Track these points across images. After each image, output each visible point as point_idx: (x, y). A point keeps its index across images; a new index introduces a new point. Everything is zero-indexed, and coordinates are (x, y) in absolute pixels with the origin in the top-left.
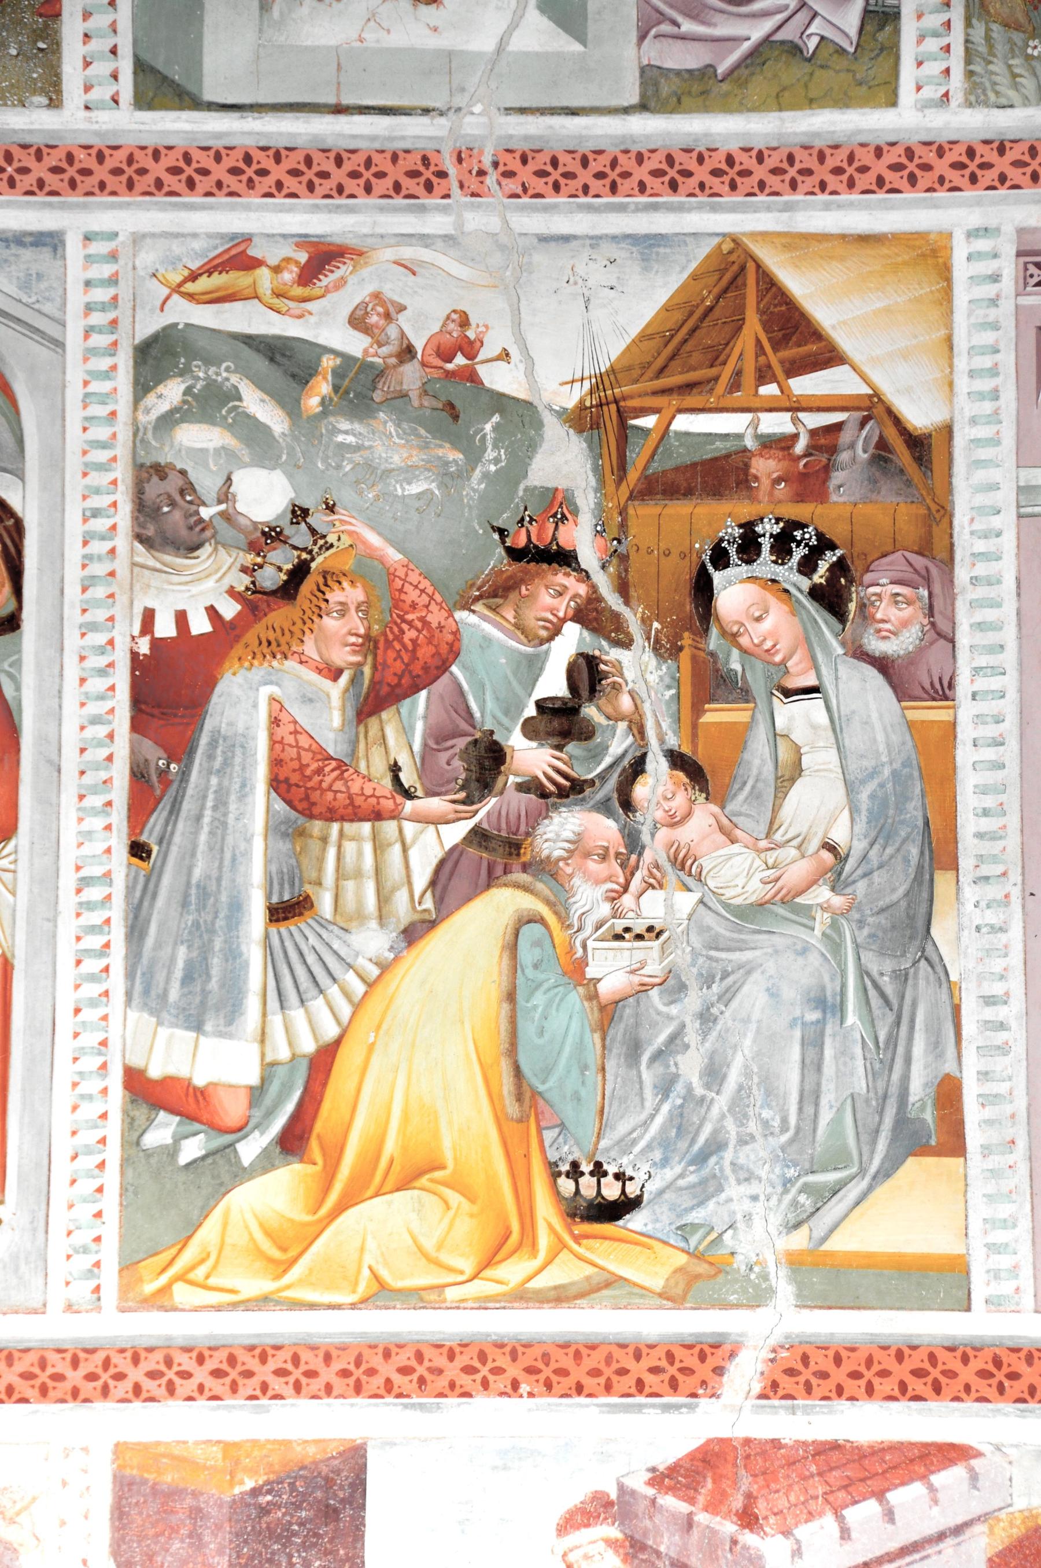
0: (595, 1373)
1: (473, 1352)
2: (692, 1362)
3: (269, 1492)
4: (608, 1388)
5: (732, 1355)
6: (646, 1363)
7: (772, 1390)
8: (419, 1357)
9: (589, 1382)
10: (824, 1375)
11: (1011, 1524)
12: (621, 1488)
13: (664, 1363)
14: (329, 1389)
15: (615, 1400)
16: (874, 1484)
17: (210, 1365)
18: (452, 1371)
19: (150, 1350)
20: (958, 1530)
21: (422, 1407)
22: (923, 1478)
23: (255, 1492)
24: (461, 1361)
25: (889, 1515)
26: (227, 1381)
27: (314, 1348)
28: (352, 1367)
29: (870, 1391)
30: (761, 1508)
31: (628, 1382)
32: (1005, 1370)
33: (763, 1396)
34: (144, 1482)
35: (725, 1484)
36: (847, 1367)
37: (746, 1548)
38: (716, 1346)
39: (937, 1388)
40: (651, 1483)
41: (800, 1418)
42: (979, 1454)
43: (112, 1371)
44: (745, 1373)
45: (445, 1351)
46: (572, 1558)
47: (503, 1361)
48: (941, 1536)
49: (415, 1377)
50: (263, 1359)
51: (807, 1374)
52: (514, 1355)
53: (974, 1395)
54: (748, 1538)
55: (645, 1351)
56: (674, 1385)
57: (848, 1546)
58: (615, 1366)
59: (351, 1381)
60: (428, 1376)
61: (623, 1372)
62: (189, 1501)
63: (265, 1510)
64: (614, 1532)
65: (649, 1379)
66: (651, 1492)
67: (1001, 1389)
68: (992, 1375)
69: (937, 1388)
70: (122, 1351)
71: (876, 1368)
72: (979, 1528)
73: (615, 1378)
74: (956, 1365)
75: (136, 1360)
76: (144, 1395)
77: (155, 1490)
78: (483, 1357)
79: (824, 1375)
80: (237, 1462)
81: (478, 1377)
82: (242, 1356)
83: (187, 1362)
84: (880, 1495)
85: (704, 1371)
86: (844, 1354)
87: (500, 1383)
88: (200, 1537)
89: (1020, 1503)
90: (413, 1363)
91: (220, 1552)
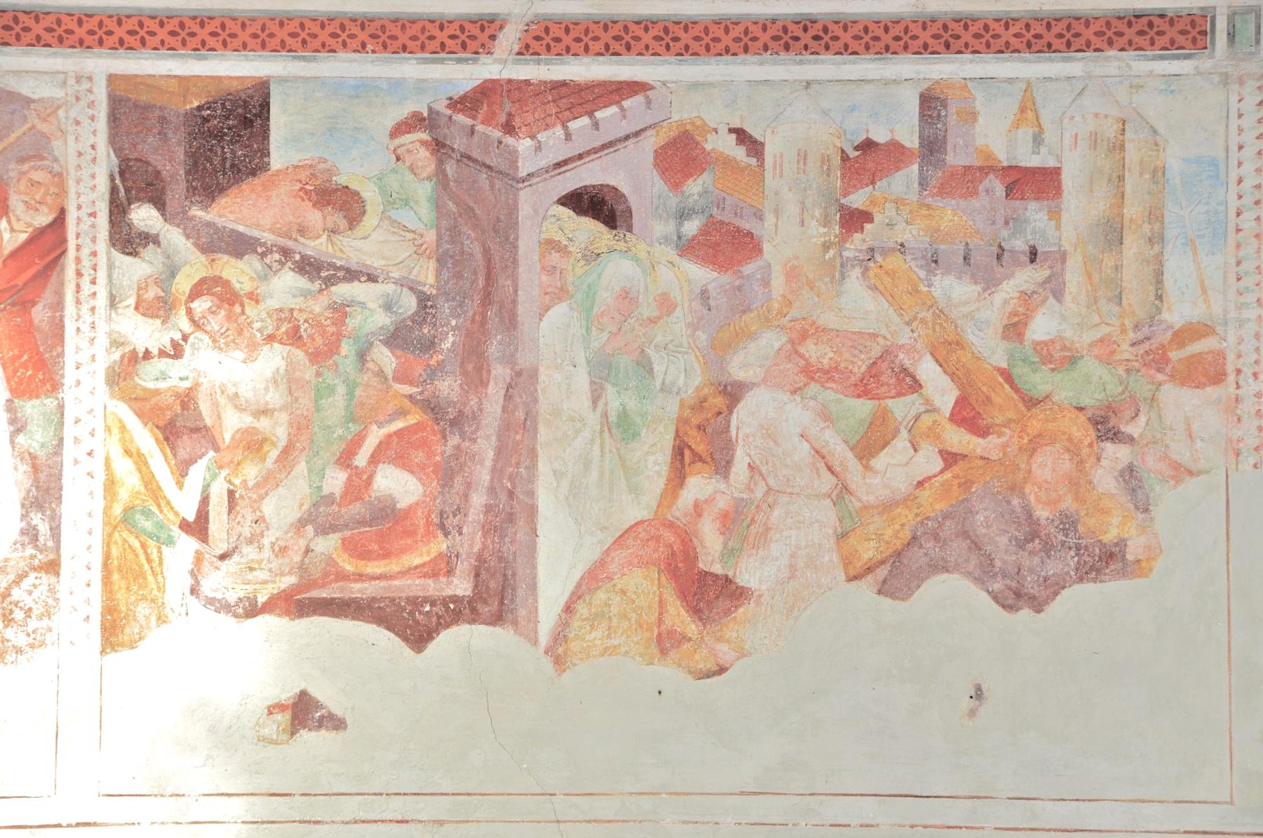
0: (414, 38)
1: (336, 24)
2: (475, 31)
3: (208, 108)
4: (423, 48)
5: (501, 28)
6: (447, 32)
7: (525, 50)
8: (302, 26)
9: (410, 44)
10: (558, 40)
11: (670, 130)
12: (430, 109)
13: (458, 33)
14: (245, 46)
15: (427, 55)
16: (588, 107)
17: (168, 28)
18: (323, 36)
19: (129, 17)
20: (637, 134)
21: (304, 59)
22: (618, 103)
23: (199, 108)
24: (329, 29)
25: (596, 125)
26: (180, 38)
27: (234, 19)
28: (259, 32)
29: (587, 49)
30: (517, 122)
31: (435, 44)
32: (671, 35)
33: (519, 53)
34: (129, 100)
35: (495, 107)
36: (573, 35)
37: (507, 146)
38: (492, 22)
39: (628, 48)
40: (449, 107)
41: (543, 68)
42: (652, 88)
43: (104, 29)
44: (509, 38)
45: (318, 23)
46: (399, 151)
47: (356, 30)
48: (627, 138)
49: (300, 39)
50: (202, 24)
51: (548, 40)
52: (363, 27)
53: (651, 51)
54: (509, 140)
55: (446, 25)
56: (464, 46)
57: (570, 144)
58: (427, 34)
59: (259, 41)
60: (307, 38)
61: (432, 38)
62: (158, 112)
63: (206, 120)
64: (425, 136)
65: (449, 42)
66: (449, 112)
67: (668, 47)
68: (663, 39)
69: (628, 48)
70: (111, 17)
71: (591, 35)
72: (649, 132)
73: (427, 42)
74: (640, 33)
75: (120, 23)
76: (126, 45)
77: (136, 105)
78: (343, 27)
79: (558, 40)
80: (188, 90)
81: (340, 40)
82: (188, 23)
83: (153, 26)
84: (590, 114)
85: (483, 37)
86: (571, 26)
87: (354, 44)
88: (165, 135)
89: (676, 117)
90: (298, 30)
91: (179, 144)
